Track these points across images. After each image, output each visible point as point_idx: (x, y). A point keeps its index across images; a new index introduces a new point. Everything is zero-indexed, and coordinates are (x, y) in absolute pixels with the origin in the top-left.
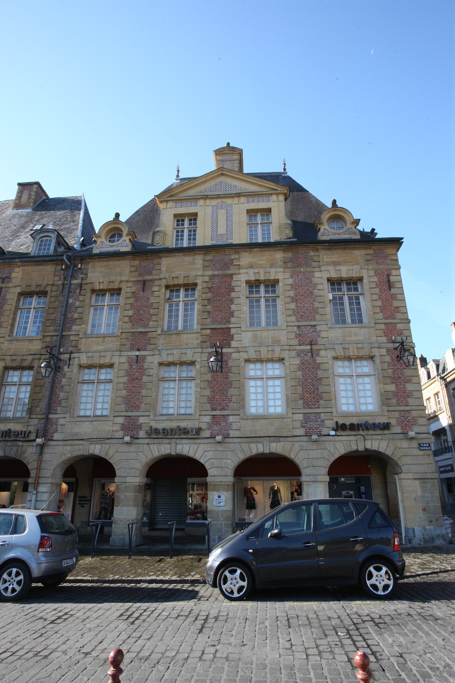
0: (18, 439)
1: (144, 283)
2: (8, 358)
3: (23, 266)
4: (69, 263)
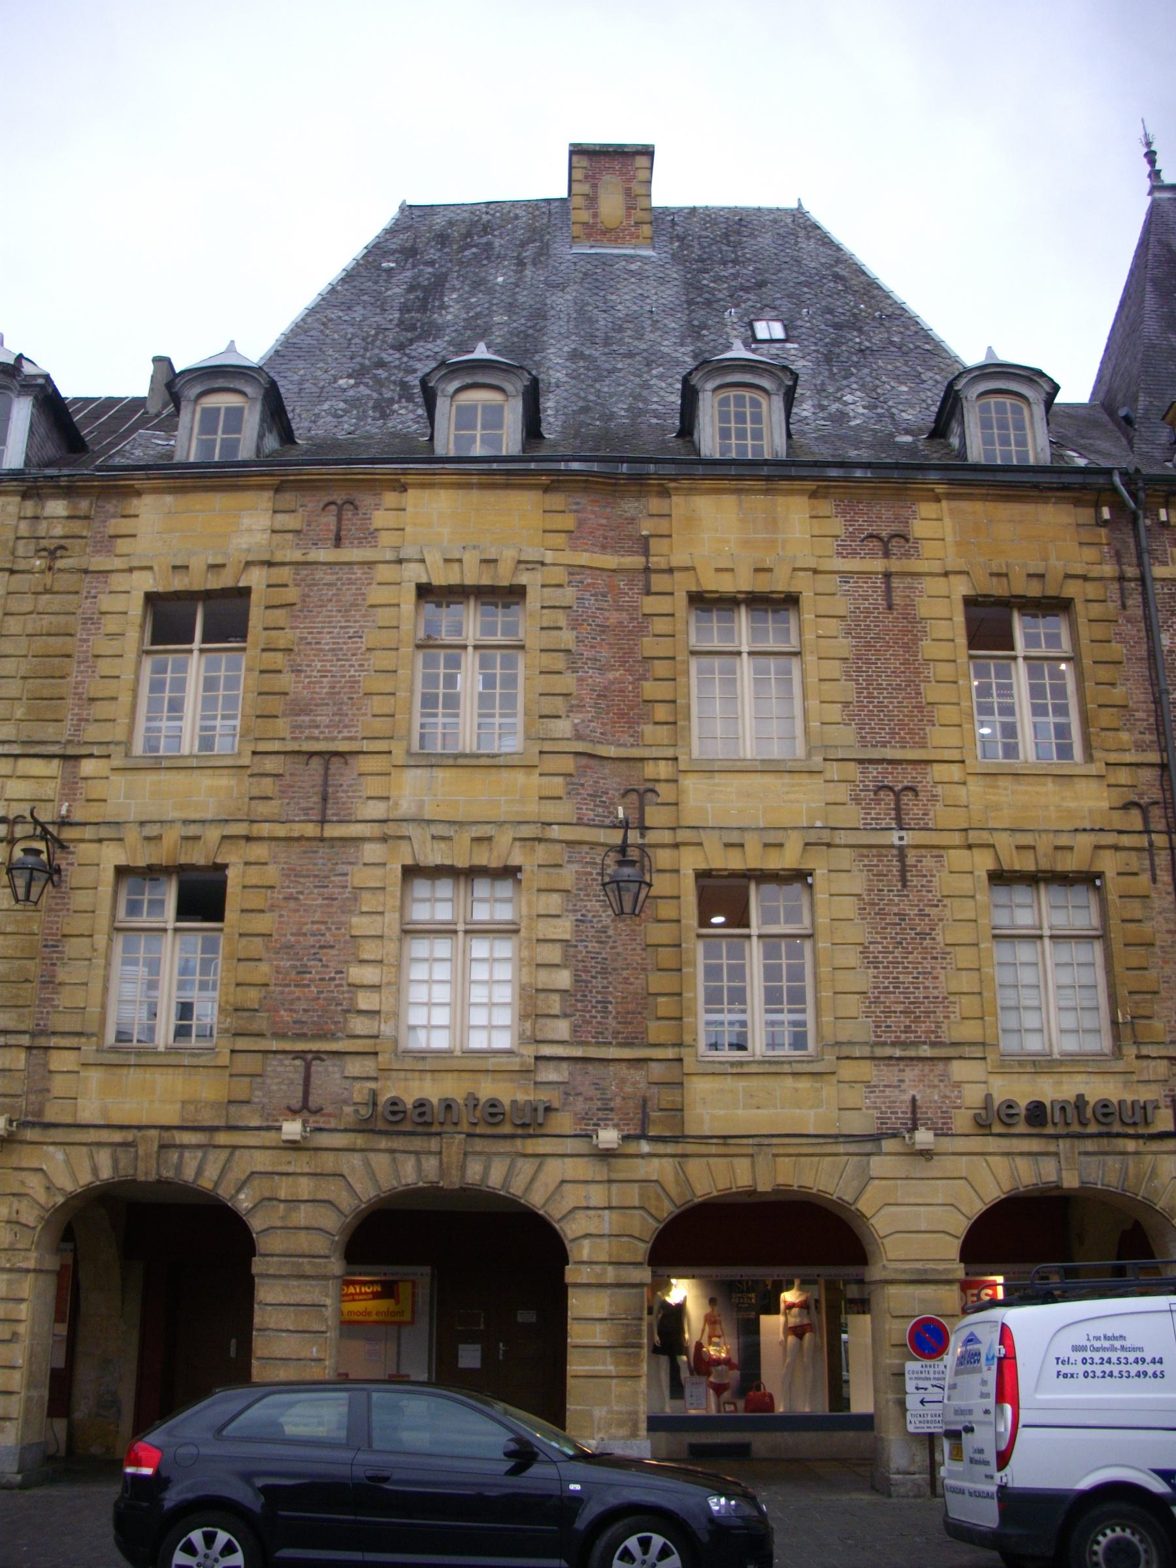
0: (1117, 1128)
2: (1004, 841)
3: (950, 497)
4: (1132, 504)
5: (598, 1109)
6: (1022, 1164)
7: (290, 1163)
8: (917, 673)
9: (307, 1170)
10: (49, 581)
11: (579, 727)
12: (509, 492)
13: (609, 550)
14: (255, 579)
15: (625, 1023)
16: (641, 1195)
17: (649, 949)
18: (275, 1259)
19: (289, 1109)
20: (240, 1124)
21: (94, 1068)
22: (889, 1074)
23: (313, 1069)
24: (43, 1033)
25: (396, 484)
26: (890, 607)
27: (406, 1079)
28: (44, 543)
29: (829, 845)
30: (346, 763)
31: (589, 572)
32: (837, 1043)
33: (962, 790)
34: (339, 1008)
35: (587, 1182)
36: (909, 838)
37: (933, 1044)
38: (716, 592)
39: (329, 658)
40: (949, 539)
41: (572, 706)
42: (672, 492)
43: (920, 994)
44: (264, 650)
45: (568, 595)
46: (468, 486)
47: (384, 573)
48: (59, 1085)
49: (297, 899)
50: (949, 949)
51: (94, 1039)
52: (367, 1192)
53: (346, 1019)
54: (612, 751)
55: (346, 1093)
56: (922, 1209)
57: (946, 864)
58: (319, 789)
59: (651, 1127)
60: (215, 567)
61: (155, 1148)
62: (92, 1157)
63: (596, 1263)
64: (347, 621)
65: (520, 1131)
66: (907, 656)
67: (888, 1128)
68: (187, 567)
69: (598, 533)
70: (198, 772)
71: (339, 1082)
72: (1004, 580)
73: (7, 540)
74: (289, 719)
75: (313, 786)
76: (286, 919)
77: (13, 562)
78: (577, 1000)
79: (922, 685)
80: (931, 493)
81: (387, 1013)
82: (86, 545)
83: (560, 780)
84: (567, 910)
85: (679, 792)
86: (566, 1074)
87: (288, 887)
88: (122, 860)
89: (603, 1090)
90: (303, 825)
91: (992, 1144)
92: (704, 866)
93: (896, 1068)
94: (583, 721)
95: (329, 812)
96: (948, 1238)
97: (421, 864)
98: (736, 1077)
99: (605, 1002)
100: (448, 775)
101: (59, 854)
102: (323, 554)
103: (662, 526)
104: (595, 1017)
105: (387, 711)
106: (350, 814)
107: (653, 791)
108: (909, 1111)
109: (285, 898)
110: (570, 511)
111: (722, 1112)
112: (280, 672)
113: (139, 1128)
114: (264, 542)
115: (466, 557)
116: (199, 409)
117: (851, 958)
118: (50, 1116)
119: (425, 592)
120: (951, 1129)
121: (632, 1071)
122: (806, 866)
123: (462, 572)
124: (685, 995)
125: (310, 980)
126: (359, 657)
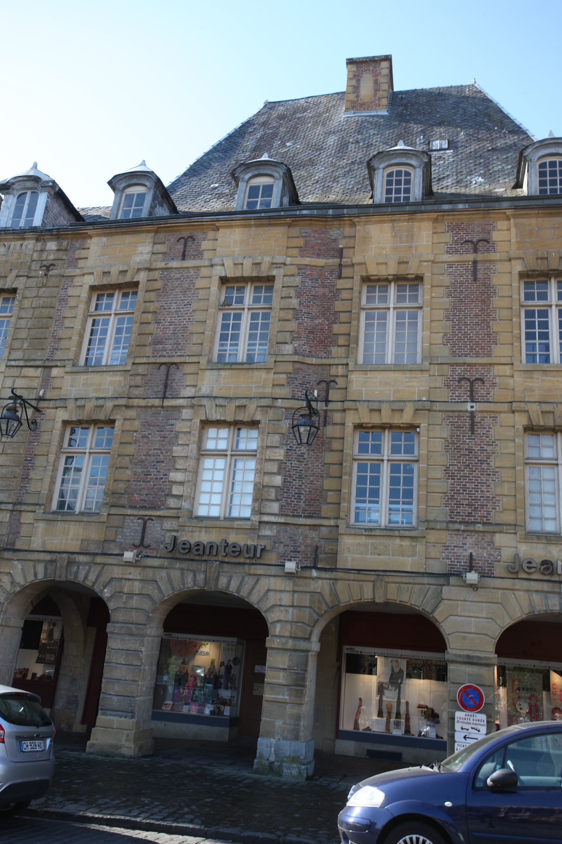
2: (534, 408)
3: (515, 216)
5: (291, 551)
6: (536, 598)
7: (131, 573)
8: (488, 315)
9: (139, 578)
10: (45, 281)
11: (297, 348)
12: (270, 228)
13: (321, 257)
14: (142, 277)
15: (309, 505)
16: (310, 600)
17: (326, 466)
18: (119, 625)
19: (134, 545)
20: (110, 552)
21: (41, 522)
22: (458, 540)
23: (148, 525)
24: (21, 504)
25: (214, 227)
26: (475, 279)
27: (192, 532)
28: (45, 263)
29: (429, 410)
30: (178, 368)
31: (309, 268)
32: (427, 521)
33: (511, 381)
34: (163, 493)
35: (281, 591)
36: (477, 407)
37: (484, 524)
38: (377, 275)
39: (174, 315)
40: (513, 240)
41: (294, 338)
42: (357, 224)
43: (479, 495)
44: (143, 313)
45: (297, 280)
46: (250, 226)
47: (204, 272)
48: (24, 530)
49: (148, 437)
50: (497, 470)
51: (43, 507)
52: (168, 592)
53: (166, 499)
54: (314, 361)
55: (162, 538)
56: (473, 619)
57: (498, 421)
58: (163, 382)
59: (319, 563)
60: (123, 272)
61: (65, 564)
62: (35, 568)
63: (283, 637)
64: (184, 297)
65: (248, 561)
66: (483, 306)
67: (454, 571)
68: (110, 272)
69: (316, 248)
70: (106, 373)
71: (159, 532)
72: (546, 261)
73: (27, 262)
74: (153, 346)
75: (161, 380)
76: (141, 447)
77: (29, 272)
78: (284, 492)
79: (491, 322)
80: (504, 215)
81: (186, 497)
82: (64, 263)
83: (284, 376)
84: (282, 444)
85: (347, 382)
86: (275, 532)
87: (144, 431)
88: (66, 417)
89: (295, 541)
90: (154, 400)
91: (519, 584)
92: (358, 421)
93: (462, 537)
94: (299, 345)
95: (167, 393)
96: (488, 638)
97: (209, 419)
98: (368, 537)
99: (299, 494)
100: (227, 374)
101: (37, 414)
102: (175, 264)
103: (351, 243)
104: (294, 502)
105: (199, 341)
106: (178, 394)
107: (334, 381)
108: (468, 561)
109: (142, 437)
110: (302, 237)
111: (359, 556)
112: (150, 323)
113: (59, 553)
114: (147, 259)
115: (245, 262)
116: (124, 195)
117: (438, 473)
118: (18, 546)
119: (224, 280)
120: (493, 574)
121: (311, 532)
122: (416, 422)
123: (242, 270)
124: (342, 491)
125: (150, 478)
126: (189, 315)
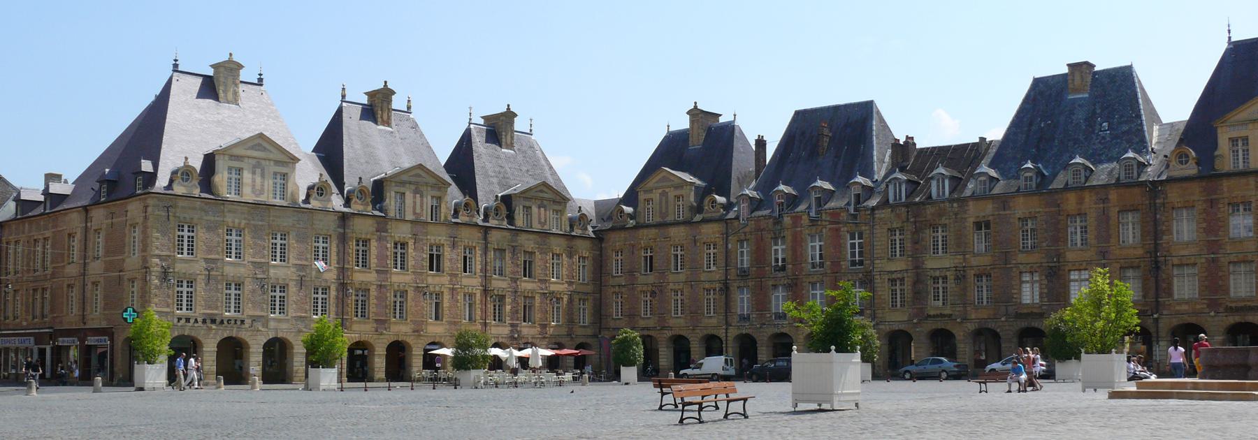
1: (1212, 201)
26: (1104, 214)
